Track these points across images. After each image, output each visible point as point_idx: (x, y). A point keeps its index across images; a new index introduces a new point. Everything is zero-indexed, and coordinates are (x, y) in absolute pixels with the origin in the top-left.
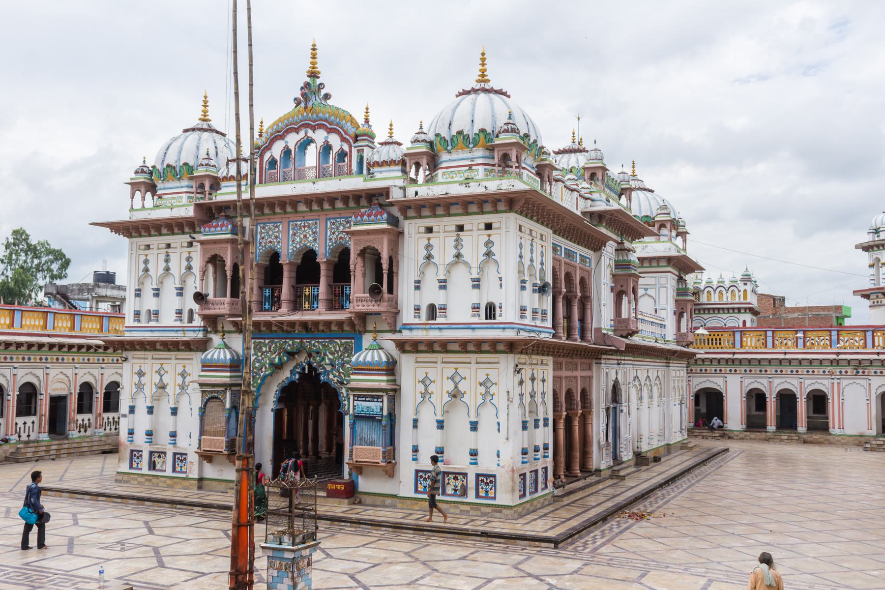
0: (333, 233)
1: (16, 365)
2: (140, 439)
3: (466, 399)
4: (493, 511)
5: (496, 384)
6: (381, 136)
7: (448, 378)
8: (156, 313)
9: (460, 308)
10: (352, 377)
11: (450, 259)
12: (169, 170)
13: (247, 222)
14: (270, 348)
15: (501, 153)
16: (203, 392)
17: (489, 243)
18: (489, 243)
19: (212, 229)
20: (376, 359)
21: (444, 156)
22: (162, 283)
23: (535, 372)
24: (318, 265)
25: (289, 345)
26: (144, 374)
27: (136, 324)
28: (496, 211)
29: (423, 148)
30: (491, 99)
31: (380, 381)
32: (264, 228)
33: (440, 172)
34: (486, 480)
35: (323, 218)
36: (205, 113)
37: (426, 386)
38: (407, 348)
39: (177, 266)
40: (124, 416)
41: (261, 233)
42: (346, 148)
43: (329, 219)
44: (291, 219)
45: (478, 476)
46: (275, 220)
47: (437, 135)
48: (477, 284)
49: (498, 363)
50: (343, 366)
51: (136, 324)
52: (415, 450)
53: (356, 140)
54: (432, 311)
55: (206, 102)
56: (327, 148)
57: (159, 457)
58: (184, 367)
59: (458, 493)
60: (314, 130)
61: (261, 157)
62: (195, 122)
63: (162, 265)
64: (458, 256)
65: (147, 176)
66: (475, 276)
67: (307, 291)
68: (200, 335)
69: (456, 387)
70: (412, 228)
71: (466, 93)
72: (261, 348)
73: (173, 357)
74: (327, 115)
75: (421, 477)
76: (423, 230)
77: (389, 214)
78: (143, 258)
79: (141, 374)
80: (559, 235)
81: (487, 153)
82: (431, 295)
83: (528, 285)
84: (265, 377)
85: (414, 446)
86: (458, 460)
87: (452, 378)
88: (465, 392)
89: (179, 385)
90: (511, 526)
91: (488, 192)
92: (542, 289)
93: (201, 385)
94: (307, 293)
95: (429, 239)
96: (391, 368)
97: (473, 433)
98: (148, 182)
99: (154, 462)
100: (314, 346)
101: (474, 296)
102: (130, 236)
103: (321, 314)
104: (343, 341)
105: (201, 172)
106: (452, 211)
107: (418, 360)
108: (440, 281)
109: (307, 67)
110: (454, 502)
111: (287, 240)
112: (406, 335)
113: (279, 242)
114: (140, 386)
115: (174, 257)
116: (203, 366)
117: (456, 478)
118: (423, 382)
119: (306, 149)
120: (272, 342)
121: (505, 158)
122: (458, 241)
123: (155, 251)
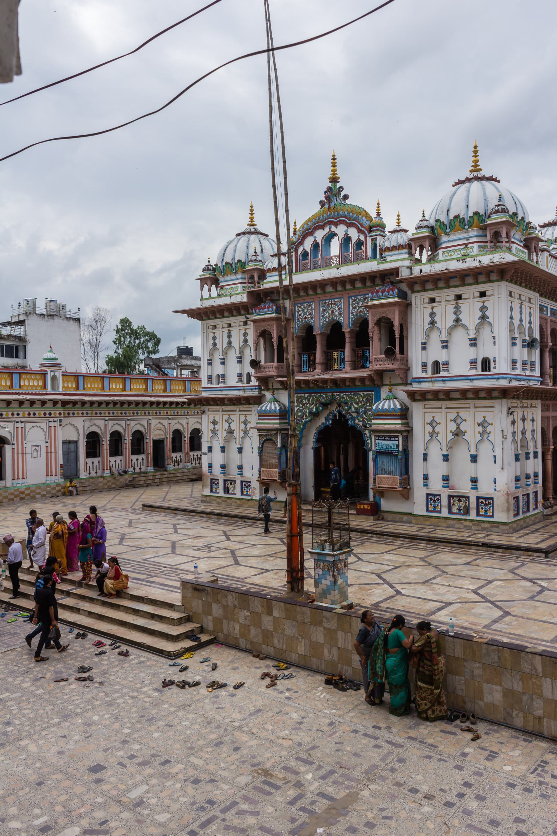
0: (355, 308)
1: (129, 418)
2: (217, 470)
3: (466, 437)
4: (492, 527)
5: (492, 424)
6: (390, 224)
7: (451, 421)
8: (224, 377)
9: (460, 363)
10: (373, 421)
11: (450, 323)
12: (227, 266)
13: (287, 303)
14: (309, 401)
15: (493, 231)
16: (260, 435)
17: (483, 309)
18: (483, 309)
19: (261, 310)
20: (392, 406)
21: (444, 238)
22: (226, 353)
23: (525, 413)
24: (343, 334)
25: (324, 398)
26: (217, 423)
27: (210, 386)
28: (489, 281)
29: (425, 233)
30: (483, 186)
31: (396, 424)
32: (300, 307)
33: (440, 252)
34: (485, 502)
35: (346, 296)
36: (252, 219)
37: (433, 428)
38: (417, 397)
39: (237, 341)
40: (205, 454)
41: (298, 311)
42: (362, 238)
43: (351, 297)
44: (321, 299)
45: (478, 498)
47: (437, 221)
48: (473, 342)
49: (493, 407)
50: (365, 413)
51: (210, 386)
52: (426, 478)
53: (370, 231)
54: (437, 366)
55: (252, 210)
56: (347, 239)
57: (231, 484)
59: (462, 512)
61: (296, 251)
62: (244, 227)
63: (226, 340)
64: (457, 320)
65: (211, 272)
66: (472, 336)
67: (335, 355)
68: (256, 392)
69: (458, 428)
70: (418, 300)
71: (461, 182)
72: (302, 401)
73: (237, 410)
74: (346, 213)
75: (431, 499)
76: (427, 300)
77: (400, 290)
78: (212, 335)
79: (215, 423)
80: (545, 297)
81: (481, 232)
82: (436, 353)
83: (518, 342)
84: (306, 423)
85: (424, 475)
86: (463, 486)
87: (455, 420)
88: (466, 432)
90: (507, 539)
91: (481, 265)
92: (530, 344)
93: (259, 430)
94: (336, 357)
95: (432, 308)
96: (404, 414)
97: (473, 464)
98: (212, 277)
99: (228, 488)
100: (343, 398)
101: (472, 353)
102: (201, 319)
103: (347, 373)
104: (365, 393)
105: (251, 266)
106: (451, 284)
107: (426, 406)
108: (443, 342)
109: (329, 174)
110: (459, 519)
111: (318, 315)
112: (416, 387)
113: (312, 318)
114: (215, 432)
115: (234, 334)
116: (259, 416)
117: (460, 500)
118: (431, 424)
119: (330, 241)
120: (310, 396)
121: (497, 235)
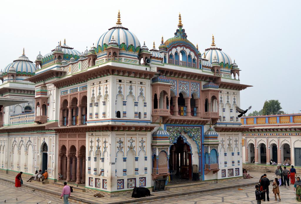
0: (193, 88)
8: (125, 113)
11: (227, 102)
12: (131, 47)
17: (234, 99)
35: (190, 82)
36: (119, 21)
43: (191, 83)
46: (174, 79)
58: (142, 138)
60: (186, 48)
64: (228, 102)
69: (230, 142)
79: (121, 142)
89: (140, 147)
94: (182, 109)
100: (188, 129)
103: (190, 117)
104: (197, 127)
110: (231, 178)
117: (230, 171)
122: (228, 97)
123: (125, 84)
